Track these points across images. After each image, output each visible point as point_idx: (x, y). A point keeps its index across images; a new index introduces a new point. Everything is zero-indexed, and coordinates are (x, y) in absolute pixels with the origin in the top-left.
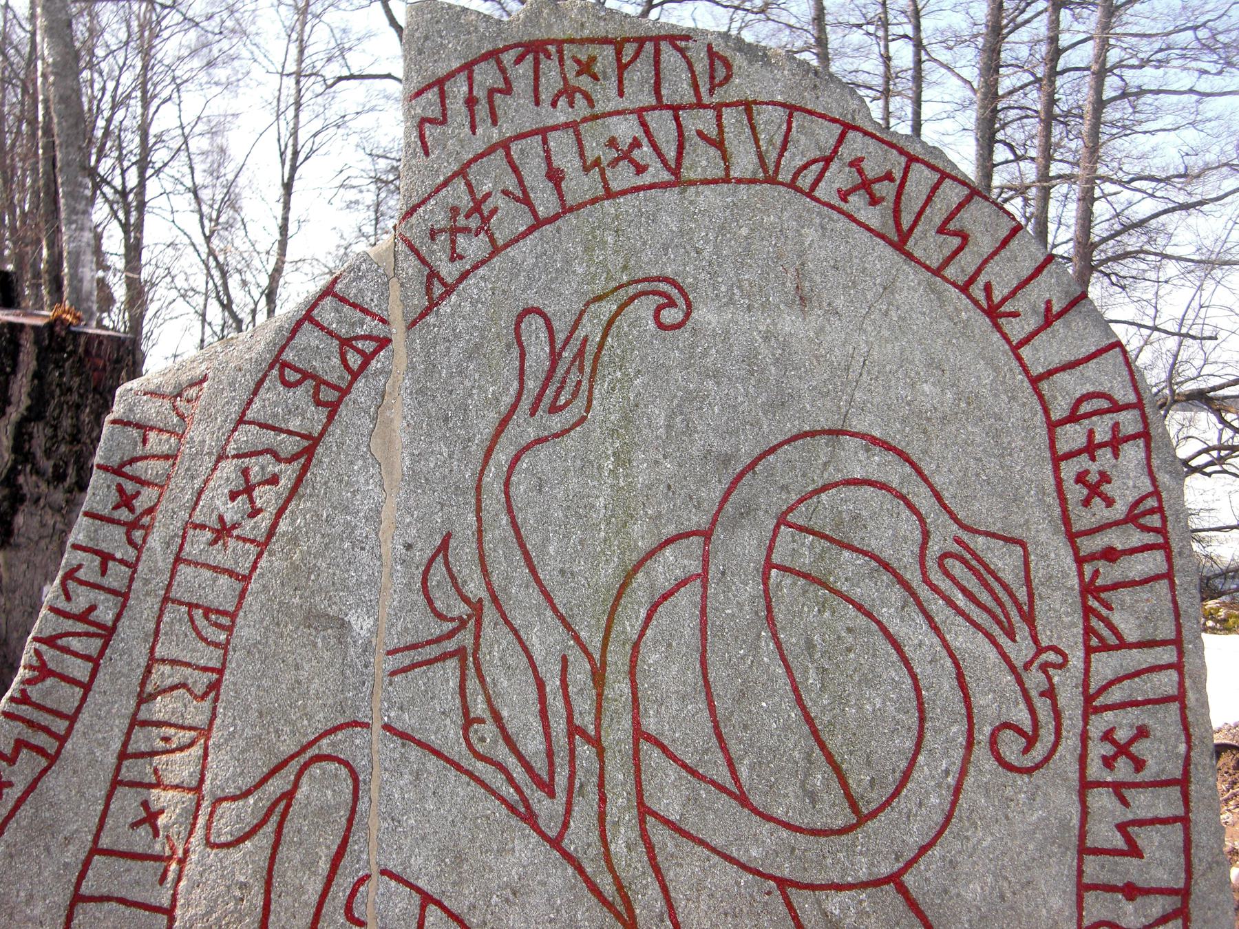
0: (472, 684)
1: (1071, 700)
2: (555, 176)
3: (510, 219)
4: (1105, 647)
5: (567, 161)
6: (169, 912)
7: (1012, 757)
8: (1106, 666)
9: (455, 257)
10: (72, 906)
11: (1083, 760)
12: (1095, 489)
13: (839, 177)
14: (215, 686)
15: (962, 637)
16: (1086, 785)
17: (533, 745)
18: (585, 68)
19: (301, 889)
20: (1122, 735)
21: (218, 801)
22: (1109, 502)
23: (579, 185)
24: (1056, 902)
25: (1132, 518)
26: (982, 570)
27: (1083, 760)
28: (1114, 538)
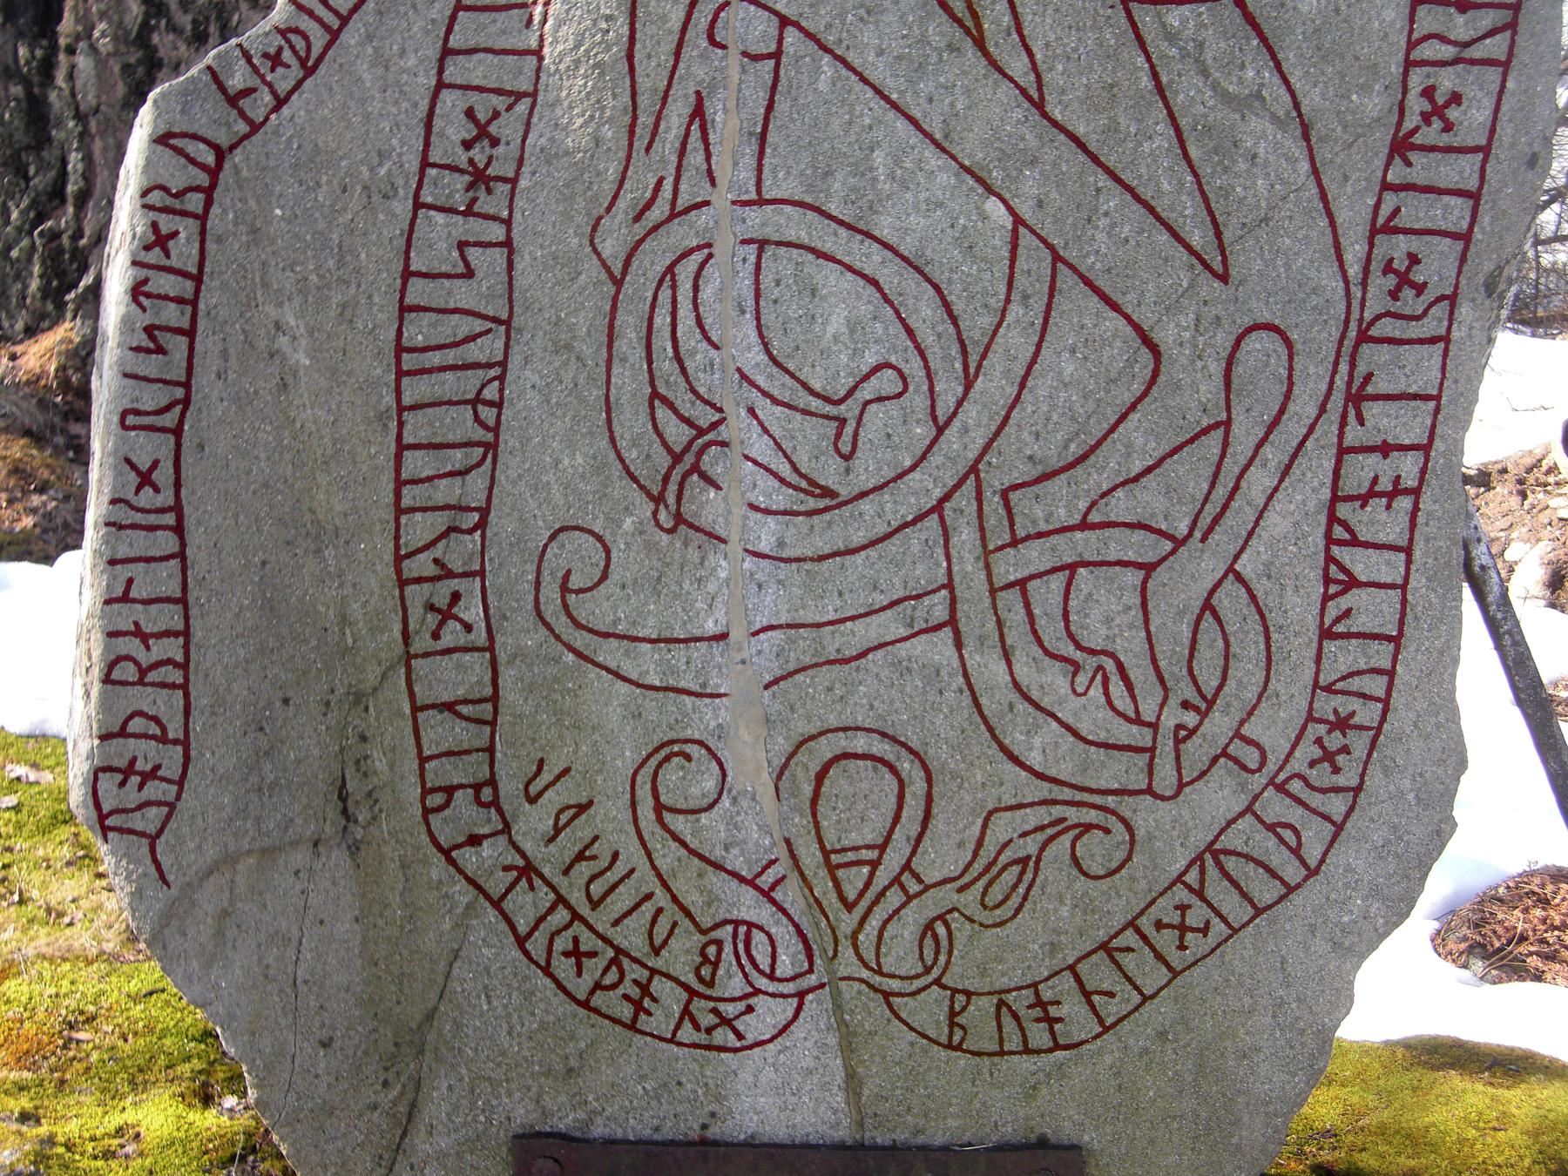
6: (538, 53)
10: (442, 61)
19: (664, 18)
24: (1389, 15)
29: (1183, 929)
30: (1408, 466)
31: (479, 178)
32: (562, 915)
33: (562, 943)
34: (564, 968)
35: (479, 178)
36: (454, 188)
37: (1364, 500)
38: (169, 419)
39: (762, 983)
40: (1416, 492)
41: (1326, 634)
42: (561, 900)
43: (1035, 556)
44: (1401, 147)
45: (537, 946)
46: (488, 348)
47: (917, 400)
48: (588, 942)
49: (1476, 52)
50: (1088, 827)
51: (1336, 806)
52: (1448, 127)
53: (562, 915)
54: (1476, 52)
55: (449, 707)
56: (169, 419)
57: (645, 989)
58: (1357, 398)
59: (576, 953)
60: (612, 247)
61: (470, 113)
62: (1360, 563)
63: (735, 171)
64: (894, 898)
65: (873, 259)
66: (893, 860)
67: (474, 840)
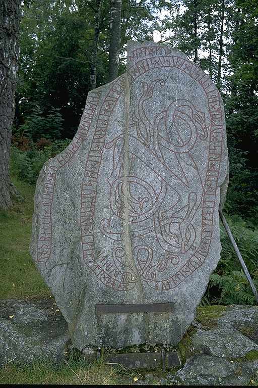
0: (138, 129)
1: (209, 133)
2: (148, 65)
3: (142, 71)
4: (214, 126)
5: (149, 63)
7: (202, 138)
8: (213, 128)
9: (135, 75)
11: (210, 139)
12: (213, 107)
13: (184, 66)
14: (106, 130)
15: (196, 124)
16: (210, 142)
17: (146, 136)
18: (152, 50)
20: (215, 136)
21: (107, 143)
22: (215, 108)
23: (151, 67)
25: (217, 111)
26: (199, 116)
27: (210, 139)
28: (215, 113)
29: (186, 272)
30: (211, 210)
31: (93, 173)
32: (102, 273)
33: (103, 276)
34: (103, 280)
35: (93, 173)
36: (89, 174)
37: (206, 214)
38: (50, 204)
39: (130, 281)
40: (213, 213)
41: (202, 232)
42: (102, 270)
43: (166, 221)
44: (208, 170)
45: (99, 277)
46: (93, 195)
47: (150, 202)
48: (107, 276)
49: (217, 159)
50: (173, 258)
51: (205, 254)
52: (214, 168)
53: (102, 273)
54: (217, 159)
55: (87, 243)
56: (50, 204)
57: (114, 282)
58: (205, 201)
59: (104, 278)
60: (111, 182)
61: (92, 164)
62: (206, 222)
63: (126, 173)
64: (148, 268)
65: (144, 184)
66: (147, 264)
67: (90, 262)
